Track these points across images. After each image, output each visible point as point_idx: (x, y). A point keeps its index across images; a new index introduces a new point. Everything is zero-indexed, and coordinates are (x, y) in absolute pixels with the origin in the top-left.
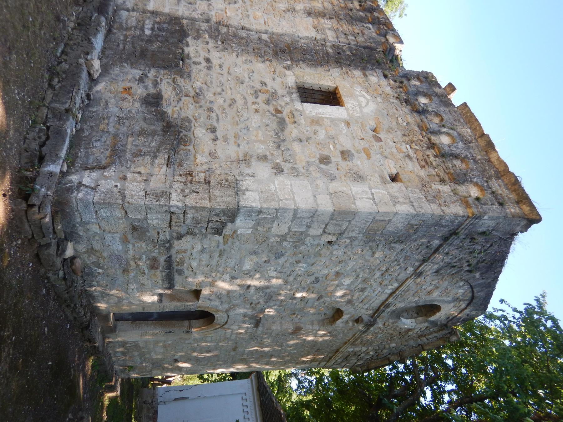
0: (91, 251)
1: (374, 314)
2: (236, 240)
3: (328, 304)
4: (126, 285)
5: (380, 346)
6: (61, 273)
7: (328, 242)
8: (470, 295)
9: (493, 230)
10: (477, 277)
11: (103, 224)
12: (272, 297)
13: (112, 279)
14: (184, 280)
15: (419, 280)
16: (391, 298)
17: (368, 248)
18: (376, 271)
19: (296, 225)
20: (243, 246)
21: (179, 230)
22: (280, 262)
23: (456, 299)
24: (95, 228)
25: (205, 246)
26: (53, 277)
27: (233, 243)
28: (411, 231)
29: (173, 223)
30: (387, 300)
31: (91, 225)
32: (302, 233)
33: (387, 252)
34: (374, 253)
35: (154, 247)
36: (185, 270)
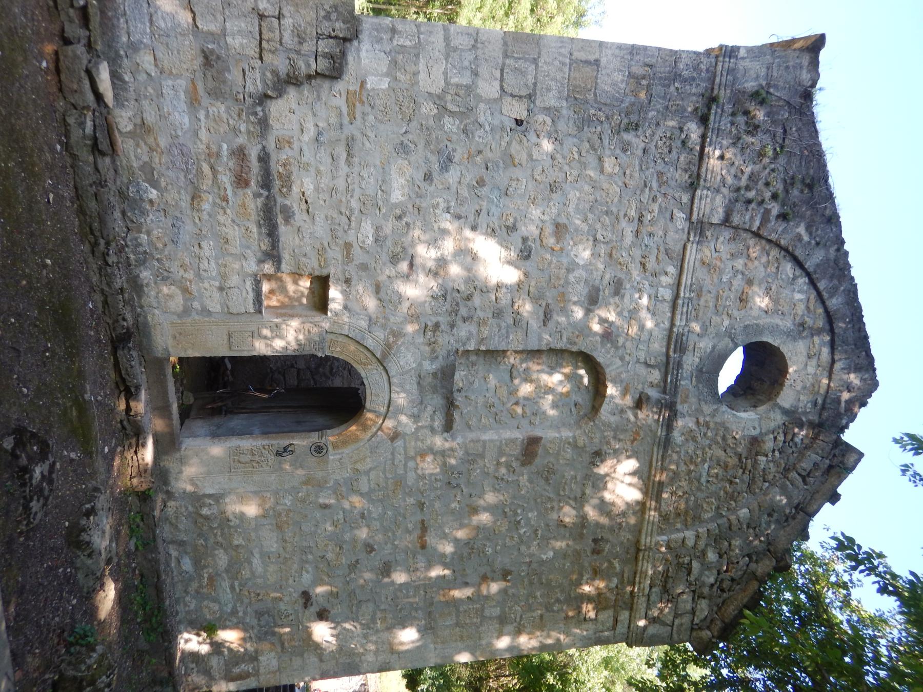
0: (143, 129)
1: (665, 381)
2: (367, 109)
3: (568, 339)
4: (197, 246)
5: (720, 522)
6: (89, 124)
7: (519, 122)
8: (820, 310)
9: (768, 85)
10: (806, 238)
11: (159, 55)
12: (457, 304)
13: (173, 226)
14: (296, 238)
15: (707, 253)
16: (678, 317)
17: (588, 146)
18: (624, 223)
19: (454, 67)
20: (382, 127)
21: (275, 63)
22: (451, 181)
23: (802, 329)
24: (146, 60)
25: (321, 125)
26: (76, 134)
27: (364, 114)
28: (642, 95)
29: (264, 44)
30: (672, 324)
31: (142, 52)
32: (469, 89)
33: (623, 158)
34: (600, 159)
35: (239, 115)
36: (295, 208)
